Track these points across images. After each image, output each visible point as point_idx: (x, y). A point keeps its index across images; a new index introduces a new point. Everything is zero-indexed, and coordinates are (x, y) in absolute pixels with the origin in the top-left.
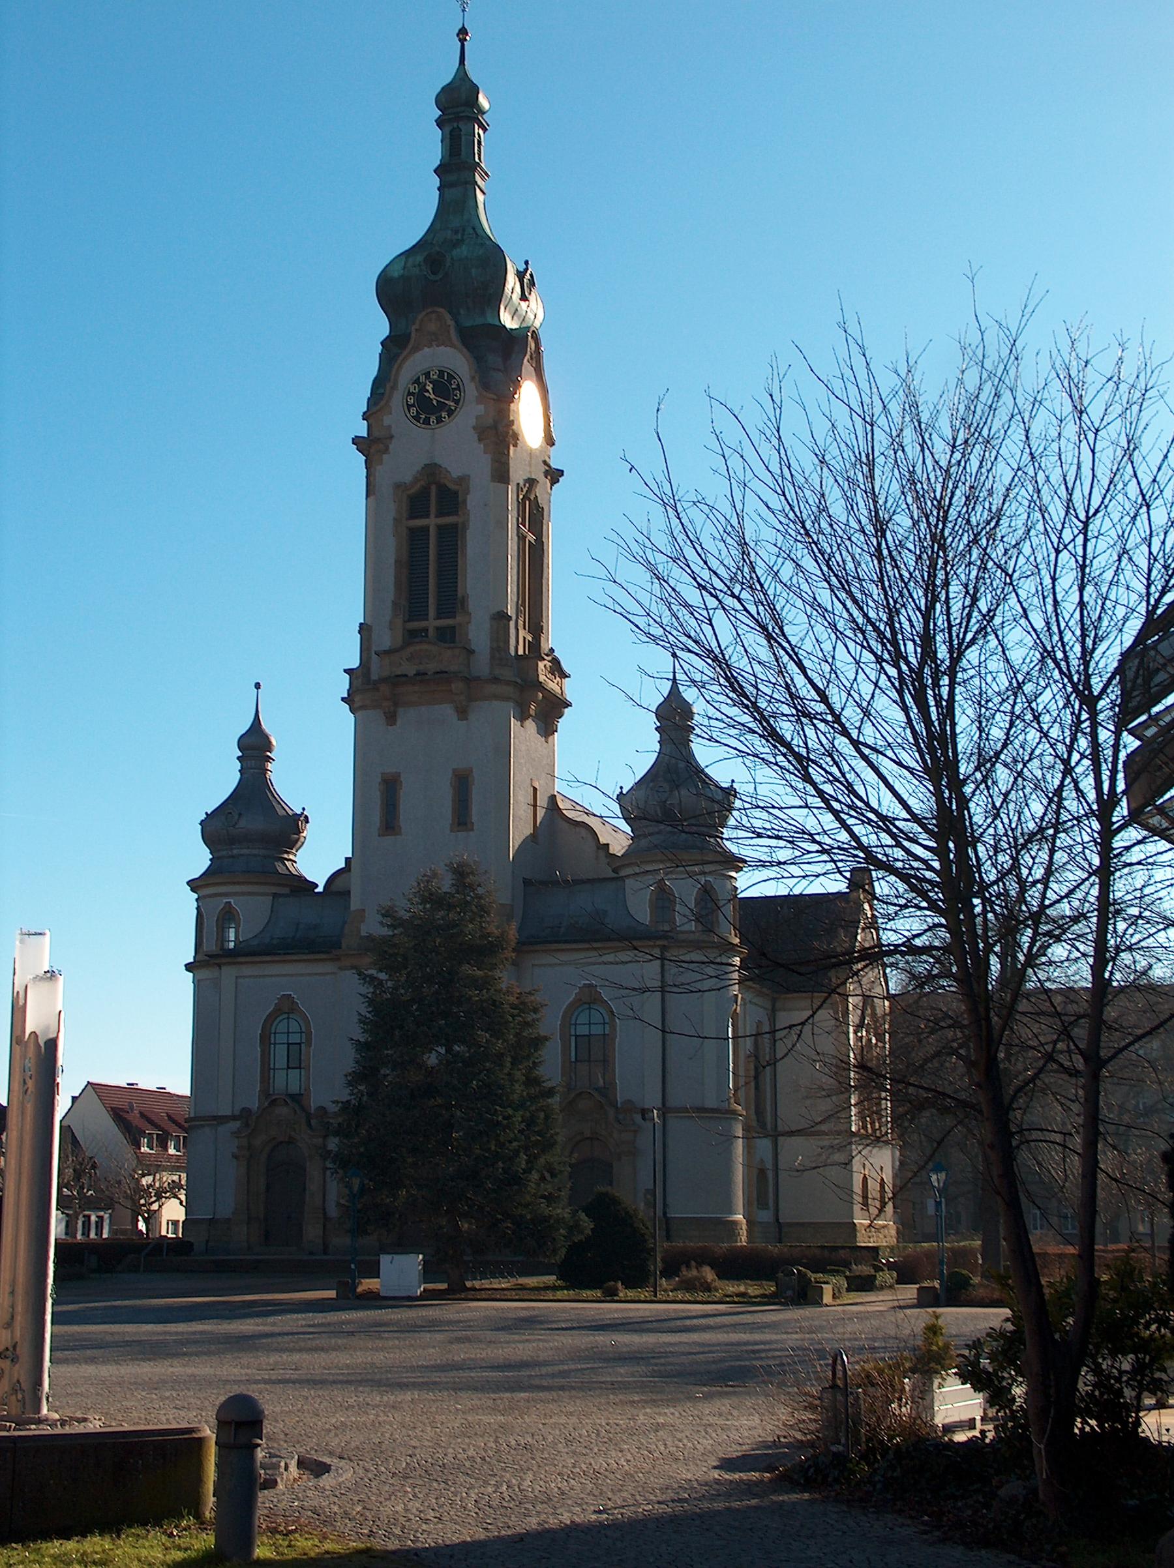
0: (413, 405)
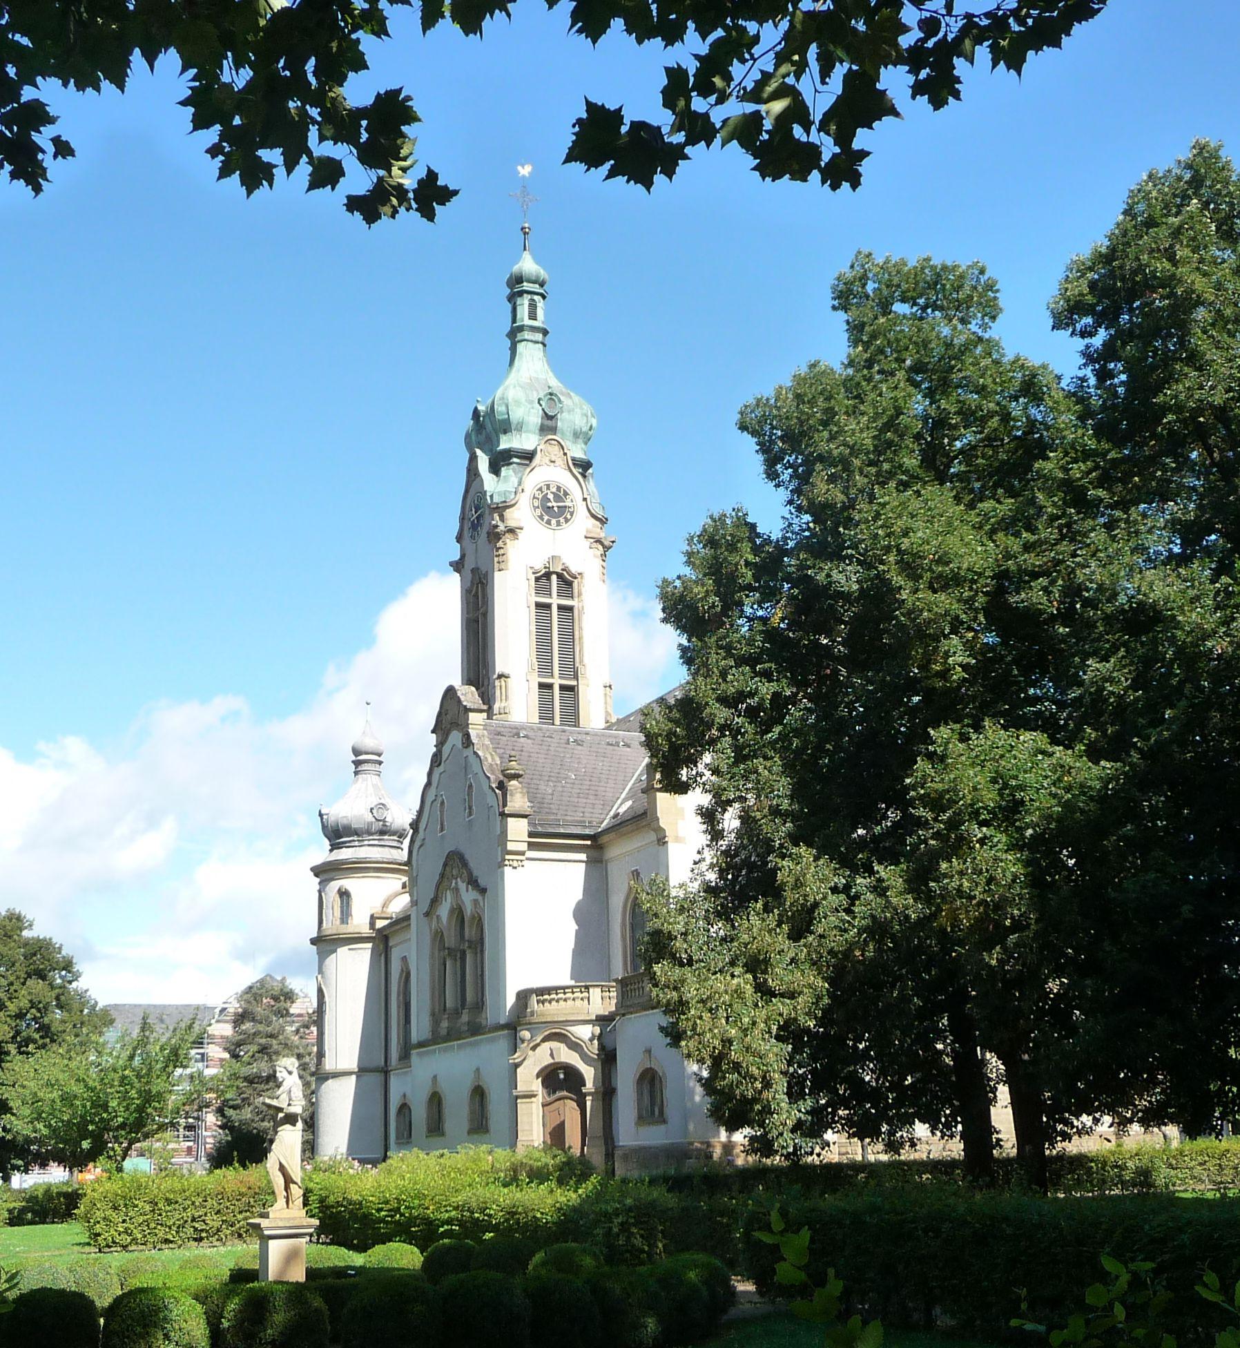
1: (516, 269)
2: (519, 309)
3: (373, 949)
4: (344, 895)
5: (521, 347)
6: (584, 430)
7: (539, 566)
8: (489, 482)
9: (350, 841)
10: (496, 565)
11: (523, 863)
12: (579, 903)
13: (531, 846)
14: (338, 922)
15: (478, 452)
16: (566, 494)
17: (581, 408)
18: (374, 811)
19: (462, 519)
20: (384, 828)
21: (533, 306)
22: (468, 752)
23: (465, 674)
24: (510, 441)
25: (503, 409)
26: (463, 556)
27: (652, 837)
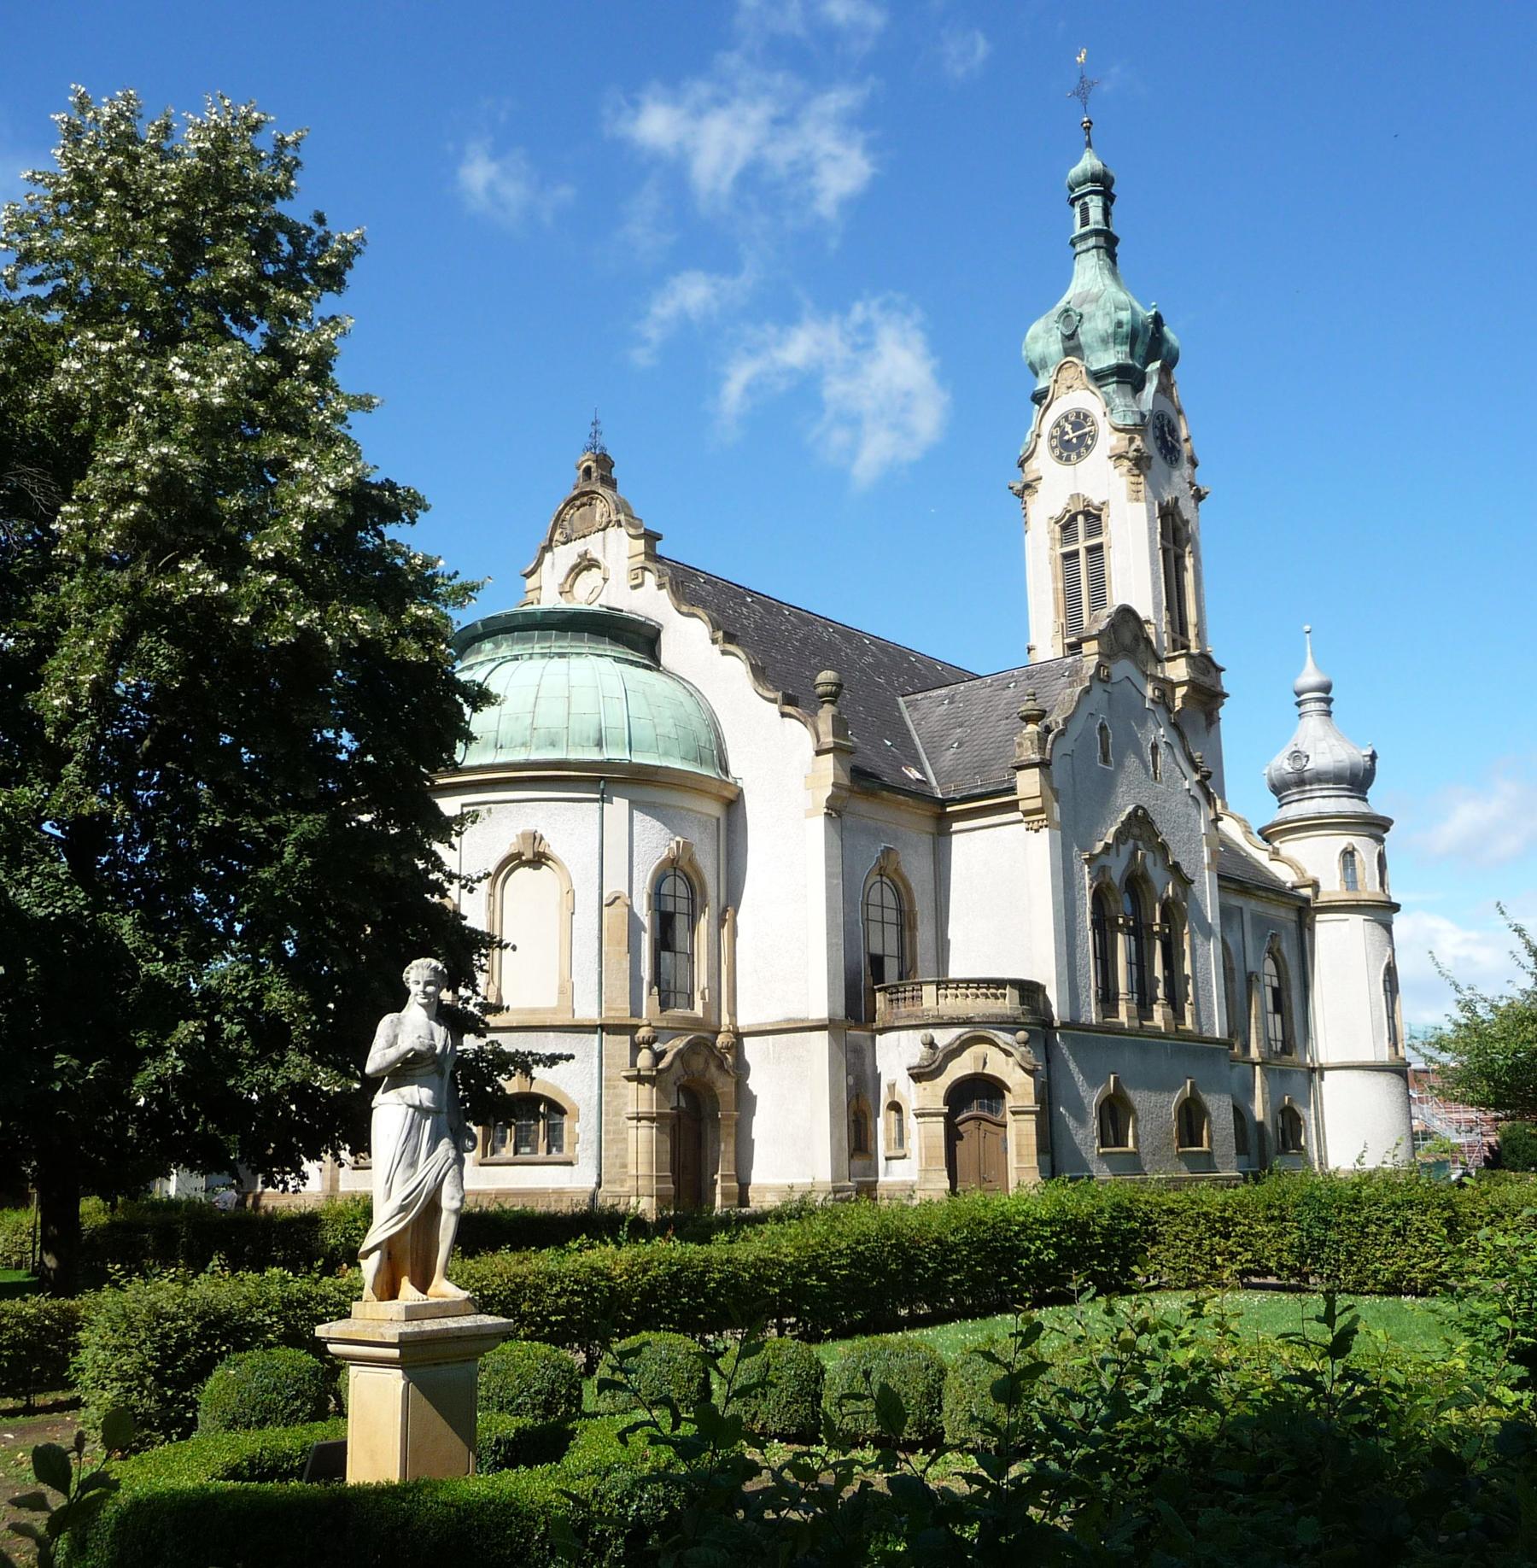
7: (1058, 512)
16: (1086, 416)
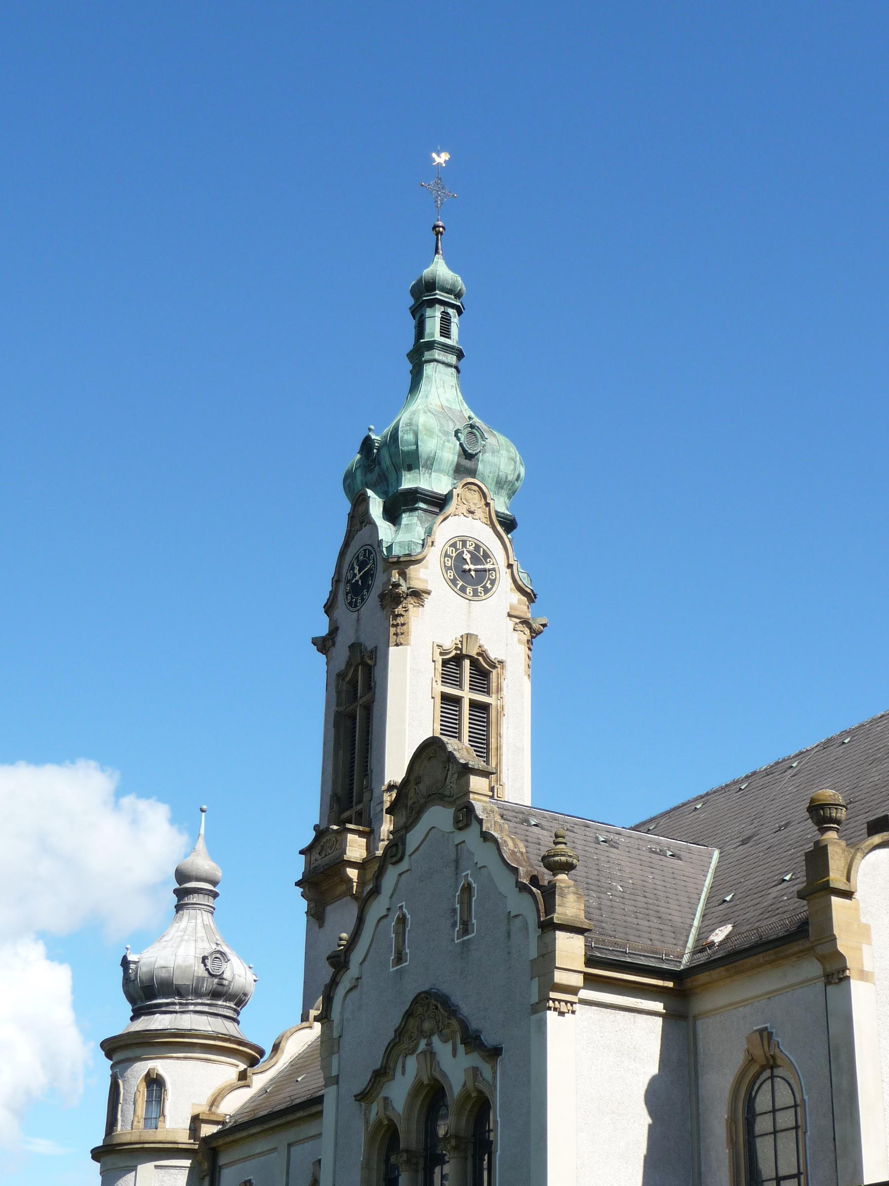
0: (450, 568)
1: (426, 272)
2: (428, 323)
3: (192, 1169)
4: (155, 1083)
5: (428, 369)
6: (510, 478)
8: (385, 531)
9: (168, 1004)
10: (392, 639)
11: (577, 1007)
12: (653, 1081)
13: (591, 981)
14: (141, 1125)
15: (370, 493)
16: (486, 556)
17: (509, 452)
18: (209, 962)
19: (336, 581)
20: (220, 988)
21: (446, 321)
22: (471, 836)
23: (330, 784)
24: (415, 480)
25: (410, 437)
26: (334, 631)
27: (812, 969)
